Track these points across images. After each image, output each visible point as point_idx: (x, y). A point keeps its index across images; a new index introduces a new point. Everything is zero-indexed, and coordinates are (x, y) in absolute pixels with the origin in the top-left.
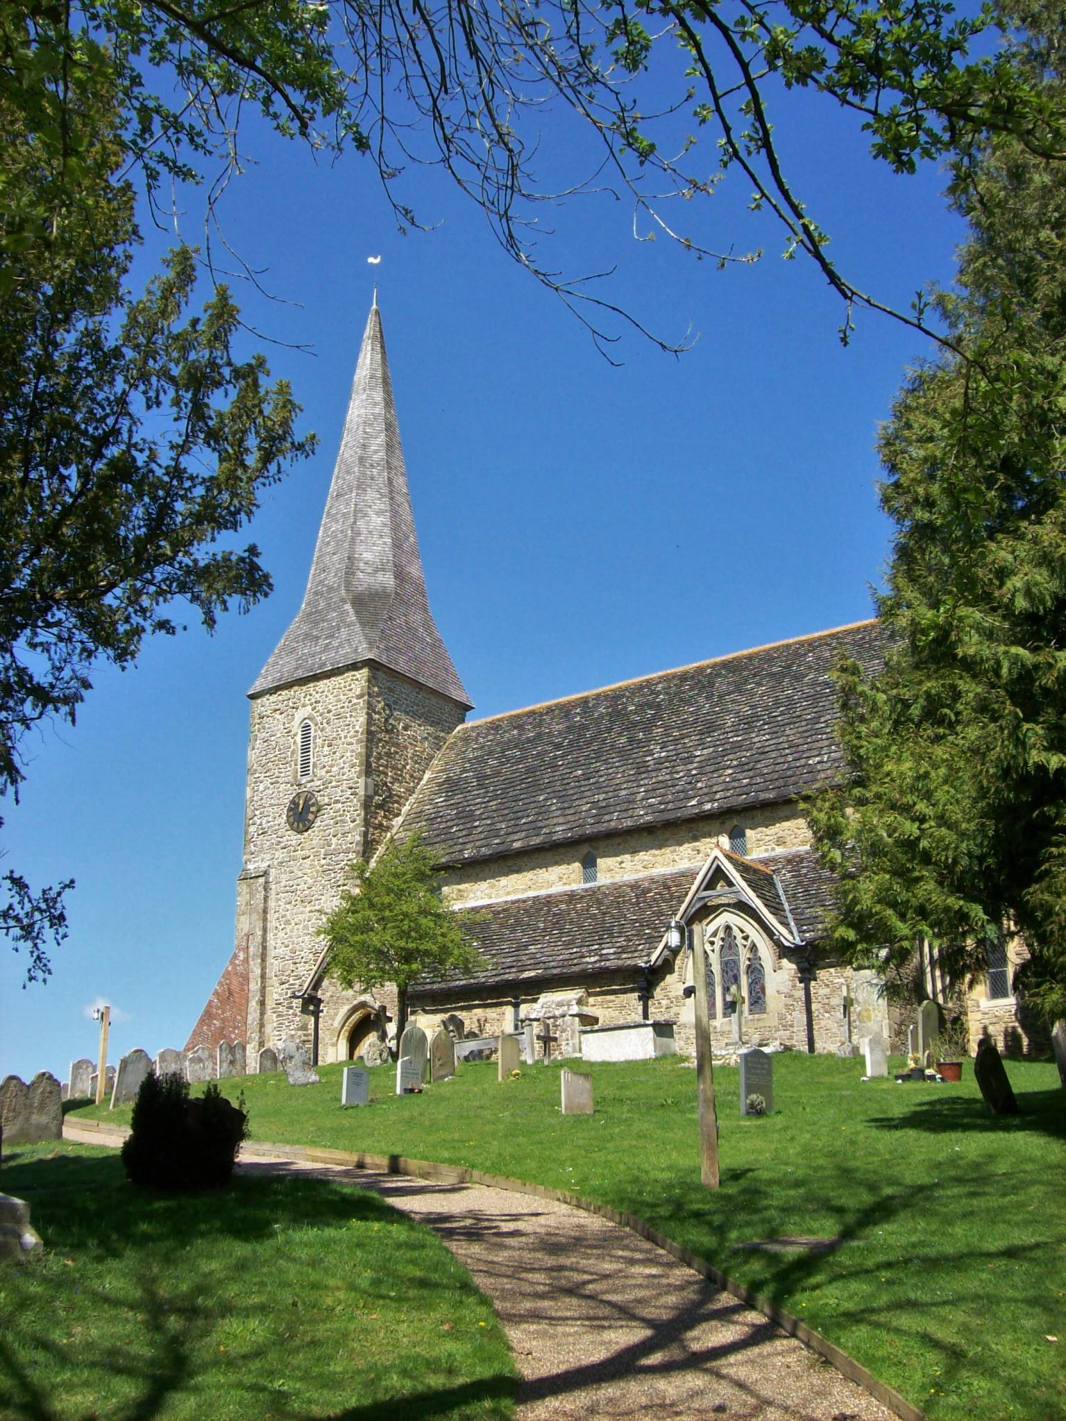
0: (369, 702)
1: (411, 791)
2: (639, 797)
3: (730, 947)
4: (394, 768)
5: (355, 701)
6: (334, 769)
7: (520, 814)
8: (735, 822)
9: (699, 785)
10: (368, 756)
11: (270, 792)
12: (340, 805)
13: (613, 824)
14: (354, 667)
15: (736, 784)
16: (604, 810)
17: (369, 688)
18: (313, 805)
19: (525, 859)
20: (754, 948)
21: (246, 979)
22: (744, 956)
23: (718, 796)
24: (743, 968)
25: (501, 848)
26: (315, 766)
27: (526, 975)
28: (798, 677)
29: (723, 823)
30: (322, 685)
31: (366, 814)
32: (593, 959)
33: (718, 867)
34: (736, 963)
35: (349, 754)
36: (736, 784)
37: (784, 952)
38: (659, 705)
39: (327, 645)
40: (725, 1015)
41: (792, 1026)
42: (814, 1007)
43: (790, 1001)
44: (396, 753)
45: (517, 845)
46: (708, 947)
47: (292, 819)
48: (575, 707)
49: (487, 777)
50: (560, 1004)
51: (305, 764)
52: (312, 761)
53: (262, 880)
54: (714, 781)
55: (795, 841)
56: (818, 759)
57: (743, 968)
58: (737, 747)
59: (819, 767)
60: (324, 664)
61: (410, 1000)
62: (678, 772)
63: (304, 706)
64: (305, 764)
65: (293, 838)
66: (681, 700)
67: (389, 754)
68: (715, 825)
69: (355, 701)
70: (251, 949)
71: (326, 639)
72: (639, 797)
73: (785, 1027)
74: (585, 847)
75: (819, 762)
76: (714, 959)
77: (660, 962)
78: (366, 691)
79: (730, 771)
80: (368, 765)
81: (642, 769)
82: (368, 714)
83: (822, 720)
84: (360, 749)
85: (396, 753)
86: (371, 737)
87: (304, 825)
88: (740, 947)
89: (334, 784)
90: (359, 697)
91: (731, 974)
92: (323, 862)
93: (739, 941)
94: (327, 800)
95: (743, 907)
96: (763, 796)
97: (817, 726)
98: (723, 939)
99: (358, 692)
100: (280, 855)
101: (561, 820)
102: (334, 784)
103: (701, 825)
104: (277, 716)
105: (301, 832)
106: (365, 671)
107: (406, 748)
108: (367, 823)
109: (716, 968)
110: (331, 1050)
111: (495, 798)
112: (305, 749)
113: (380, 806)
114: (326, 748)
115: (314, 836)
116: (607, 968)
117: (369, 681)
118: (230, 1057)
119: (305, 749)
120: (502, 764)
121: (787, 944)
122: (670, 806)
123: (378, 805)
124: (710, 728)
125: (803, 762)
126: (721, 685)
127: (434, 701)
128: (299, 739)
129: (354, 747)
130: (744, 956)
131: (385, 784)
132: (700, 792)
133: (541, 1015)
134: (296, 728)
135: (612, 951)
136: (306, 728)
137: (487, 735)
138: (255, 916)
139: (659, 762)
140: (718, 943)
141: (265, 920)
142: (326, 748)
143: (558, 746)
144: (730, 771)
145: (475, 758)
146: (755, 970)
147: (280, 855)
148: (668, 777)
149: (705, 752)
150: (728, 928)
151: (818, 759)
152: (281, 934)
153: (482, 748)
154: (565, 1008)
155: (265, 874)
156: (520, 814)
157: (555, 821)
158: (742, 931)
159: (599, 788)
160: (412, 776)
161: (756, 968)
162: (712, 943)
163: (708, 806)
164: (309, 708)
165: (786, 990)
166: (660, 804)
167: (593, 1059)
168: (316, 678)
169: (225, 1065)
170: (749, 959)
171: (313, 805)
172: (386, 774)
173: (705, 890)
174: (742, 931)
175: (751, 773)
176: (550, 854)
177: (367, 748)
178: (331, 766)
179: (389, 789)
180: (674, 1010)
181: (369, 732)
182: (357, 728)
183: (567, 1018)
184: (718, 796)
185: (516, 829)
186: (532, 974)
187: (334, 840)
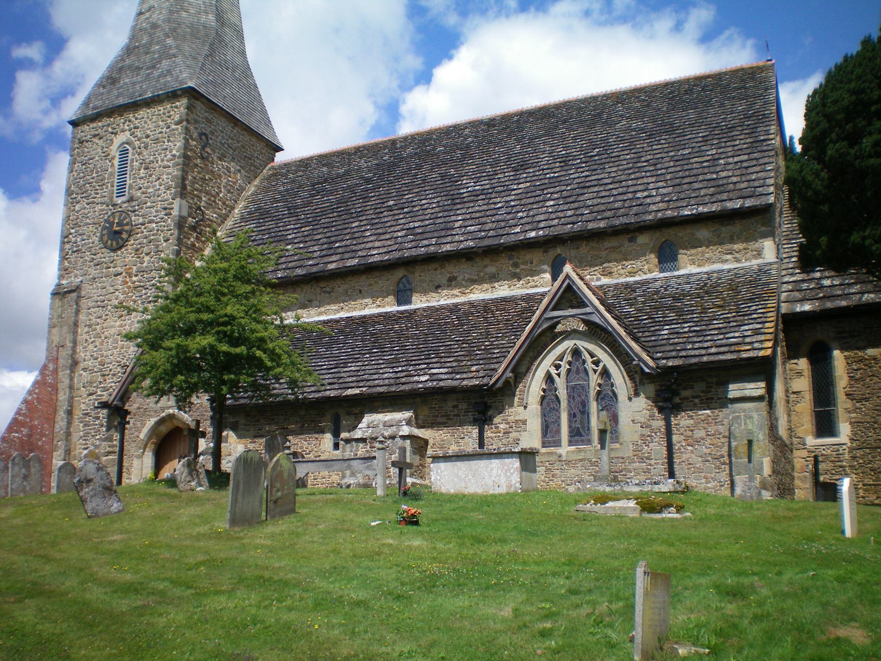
0: (187, 129)
1: (224, 218)
2: (457, 225)
3: (578, 372)
4: (207, 193)
5: (174, 127)
6: (150, 190)
7: (333, 239)
8: (559, 251)
9: (520, 214)
10: (184, 179)
11: (86, 211)
12: (154, 225)
13: (432, 248)
14: (173, 95)
15: (561, 215)
16: (418, 236)
17: (187, 114)
18: (127, 224)
19: (339, 282)
20: (605, 373)
21: (56, 390)
22: (594, 379)
23: (542, 225)
24: (592, 394)
25: (315, 269)
26: (131, 187)
27: (350, 392)
28: (609, 124)
29: (546, 252)
30: (142, 113)
31: (180, 234)
32: (423, 378)
33: (569, 288)
34: (585, 389)
35: (165, 177)
36: (561, 215)
37: (639, 378)
38: (468, 147)
39: (148, 75)
40: (570, 443)
41: (648, 458)
42: (675, 438)
43: (647, 432)
44: (211, 180)
45: (332, 266)
46: (553, 371)
47: (105, 238)
48: (385, 147)
49: (296, 207)
50: (388, 425)
51: (122, 186)
52: (128, 182)
53: (74, 295)
54: (535, 211)
55: (622, 271)
56: (646, 194)
57: (592, 394)
58: (555, 182)
59: (648, 200)
60: (145, 92)
61: (224, 417)
62: (495, 203)
63: (123, 131)
64: (122, 186)
65: (106, 255)
66: (490, 142)
67: (203, 179)
68: (536, 255)
69: (174, 127)
70: (61, 362)
71: (148, 68)
72: (457, 225)
73: (642, 460)
74: (402, 272)
75: (646, 197)
76: (560, 383)
77: (499, 384)
78: (184, 117)
79: (552, 203)
80: (184, 187)
81: (456, 200)
82: (186, 139)
83: (643, 159)
84: (176, 172)
85: (211, 180)
86: (186, 161)
87: (118, 244)
88: (591, 373)
89: (149, 204)
90: (177, 124)
91: (578, 399)
92: (134, 279)
93: (590, 366)
94: (141, 220)
95: (596, 331)
96: (591, 226)
97: (639, 165)
98: (570, 363)
99: (177, 118)
100: (93, 272)
101: (377, 244)
102: (149, 204)
103: (522, 253)
104: (96, 140)
105: (114, 250)
106: (184, 101)
107: (220, 176)
108: (180, 242)
109: (562, 393)
110: (136, 463)
111: (308, 224)
112: (122, 173)
113: (193, 228)
114: (142, 171)
115: (127, 255)
116: (441, 388)
117: (188, 108)
118: (23, 471)
119: (122, 173)
120: (312, 196)
121: (647, 370)
122: (491, 233)
123: (191, 228)
124: (523, 166)
125: (630, 196)
126: (530, 130)
127: (247, 137)
128: (116, 162)
129: (170, 170)
130: (594, 379)
131: (199, 208)
132: (523, 221)
133: (367, 435)
134: (114, 150)
135: (442, 370)
136: (124, 153)
137: (296, 171)
138: (65, 329)
139: (475, 194)
140: (564, 367)
141: (75, 333)
142: (142, 171)
143: (368, 181)
144: (552, 203)
145: (287, 190)
146: (607, 398)
147: (93, 272)
148: (485, 207)
149: (521, 186)
150: (576, 352)
151: (646, 194)
152: (91, 347)
153: (293, 182)
154: (394, 429)
155: (77, 289)
156: (333, 239)
157: (370, 245)
158: (592, 355)
159: (413, 215)
160: (224, 203)
161: (606, 395)
162: (558, 367)
163: (533, 234)
164: (128, 133)
165: (643, 420)
166: (480, 231)
167: (444, 490)
168: (135, 106)
169: (18, 480)
170: (600, 385)
171: (127, 224)
172: (200, 198)
173: (554, 309)
174: (592, 355)
175: (576, 205)
176: (364, 277)
177: (183, 170)
178: (148, 188)
179: (203, 213)
180: (514, 435)
181: (185, 156)
182: (174, 152)
183: (398, 439)
184: (542, 225)
185: (330, 251)
186: (357, 391)
187: (147, 258)
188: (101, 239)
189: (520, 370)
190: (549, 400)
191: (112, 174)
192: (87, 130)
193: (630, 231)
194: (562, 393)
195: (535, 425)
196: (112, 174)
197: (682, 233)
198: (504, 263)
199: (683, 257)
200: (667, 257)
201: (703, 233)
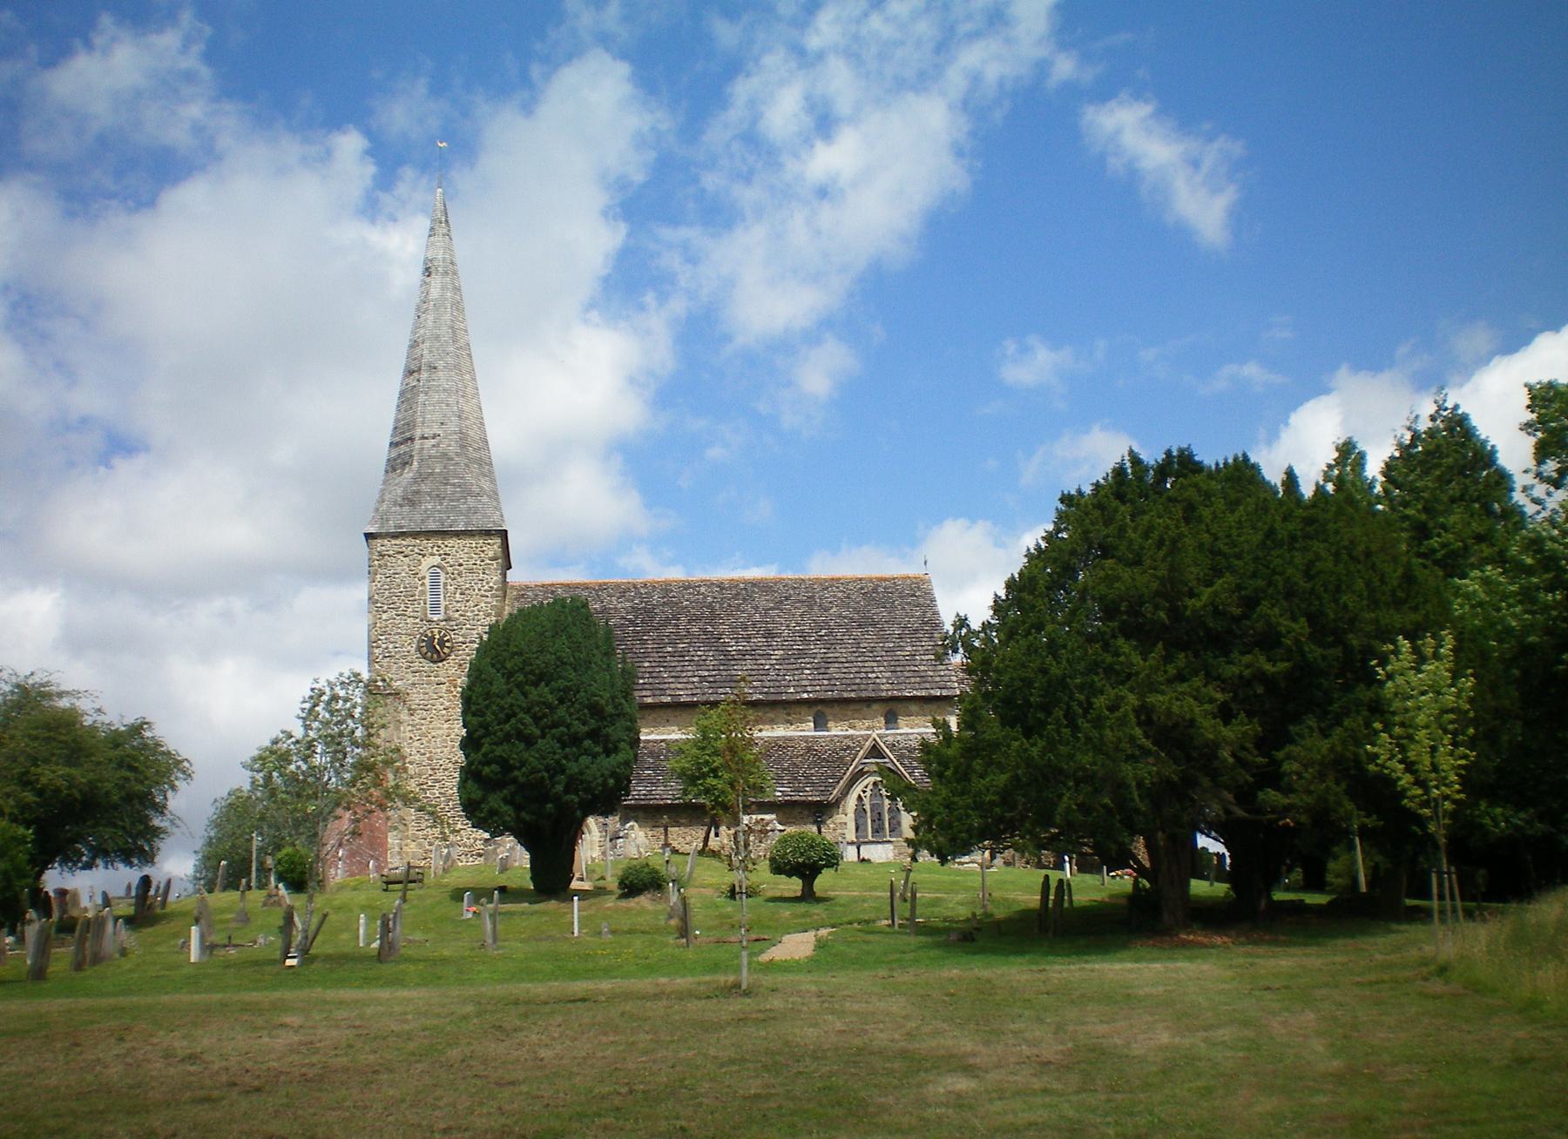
30: (451, 542)
51: (435, 607)
65: (427, 665)
68: (804, 710)
76: (866, 801)
99: (491, 554)
109: (868, 807)
136: (435, 576)
140: (868, 793)
152: (417, 744)
188: (419, 649)
189: (846, 792)
190: (860, 811)
191: (423, 593)
192: (388, 545)
193: (869, 701)
194: (868, 807)
195: (852, 826)
196: (423, 593)
197: (899, 707)
198: (782, 714)
199: (902, 721)
200: (891, 720)
201: (914, 708)
